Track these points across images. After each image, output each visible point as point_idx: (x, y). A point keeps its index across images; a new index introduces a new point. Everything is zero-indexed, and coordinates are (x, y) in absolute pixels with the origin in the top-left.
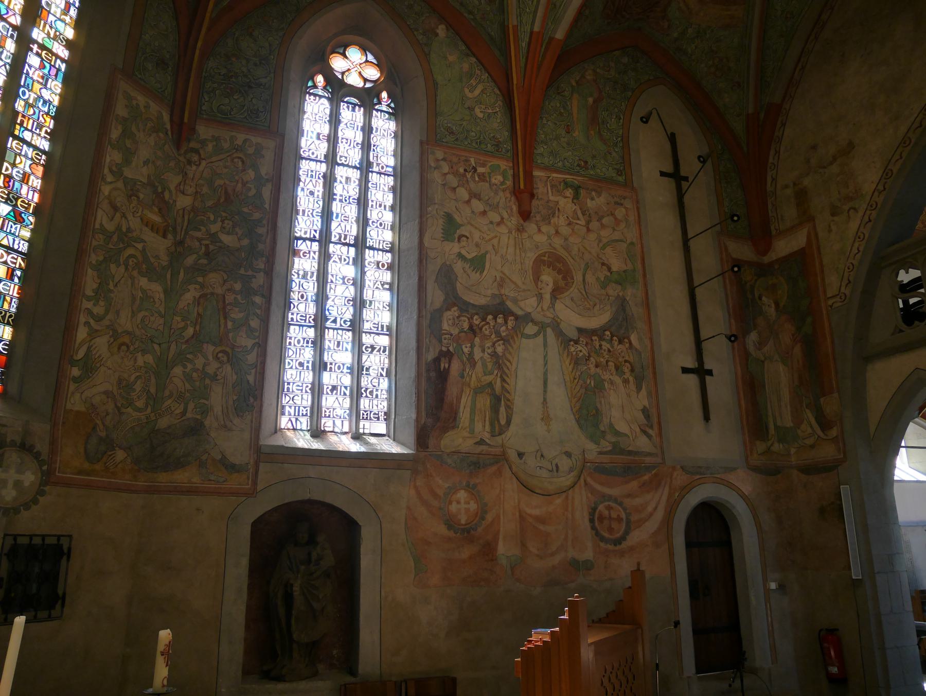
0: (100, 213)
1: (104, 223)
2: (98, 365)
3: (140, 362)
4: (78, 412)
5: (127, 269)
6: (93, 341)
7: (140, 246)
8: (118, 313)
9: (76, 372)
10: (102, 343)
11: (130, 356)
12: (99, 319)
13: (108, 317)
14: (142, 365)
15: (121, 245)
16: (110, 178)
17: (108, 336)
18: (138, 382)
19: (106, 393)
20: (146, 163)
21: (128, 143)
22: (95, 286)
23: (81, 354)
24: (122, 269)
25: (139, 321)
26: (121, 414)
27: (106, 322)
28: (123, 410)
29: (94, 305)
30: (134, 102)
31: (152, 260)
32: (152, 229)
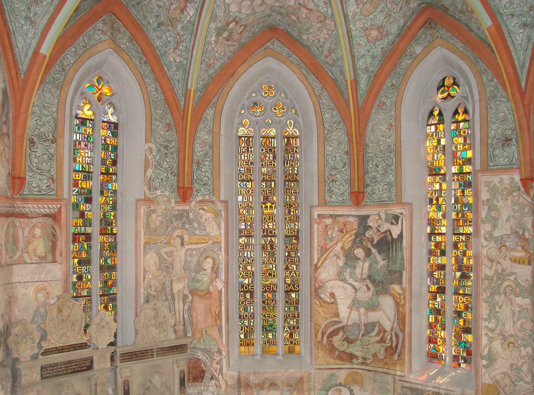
0: (484, 267)
1: (487, 273)
2: (497, 357)
3: (524, 353)
4: (489, 384)
5: (506, 295)
6: (491, 344)
7: (512, 278)
8: (504, 324)
9: (484, 362)
10: (497, 345)
11: (516, 349)
12: (492, 330)
13: (498, 328)
14: (525, 354)
15: (500, 282)
16: (485, 243)
17: (499, 340)
18: (525, 366)
19: (504, 373)
20: (508, 220)
21: (493, 214)
22: (488, 311)
23: (485, 352)
24: (503, 296)
25: (519, 326)
26: (515, 385)
27: (497, 331)
28: (516, 383)
29: (489, 323)
30: (492, 185)
31: (523, 284)
32: (519, 263)
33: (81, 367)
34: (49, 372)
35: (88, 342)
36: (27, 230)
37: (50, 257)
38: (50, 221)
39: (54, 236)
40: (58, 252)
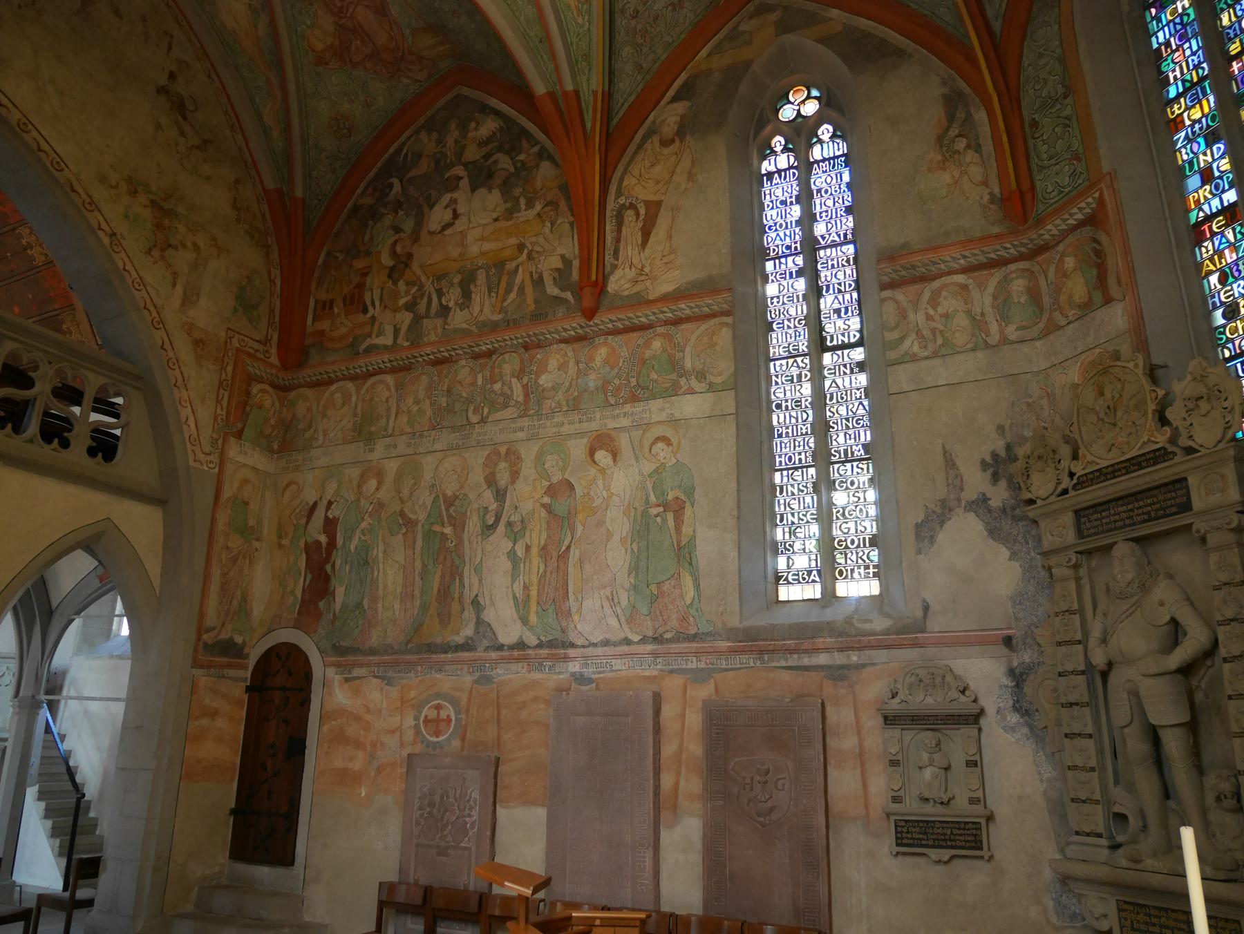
33: (1164, 509)
34: (1095, 523)
35: (1168, 446)
36: (1052, 269)
37: (1098, 297)
38: (1087, 231)
39: (1099, 253)
40: (1112, 281)
